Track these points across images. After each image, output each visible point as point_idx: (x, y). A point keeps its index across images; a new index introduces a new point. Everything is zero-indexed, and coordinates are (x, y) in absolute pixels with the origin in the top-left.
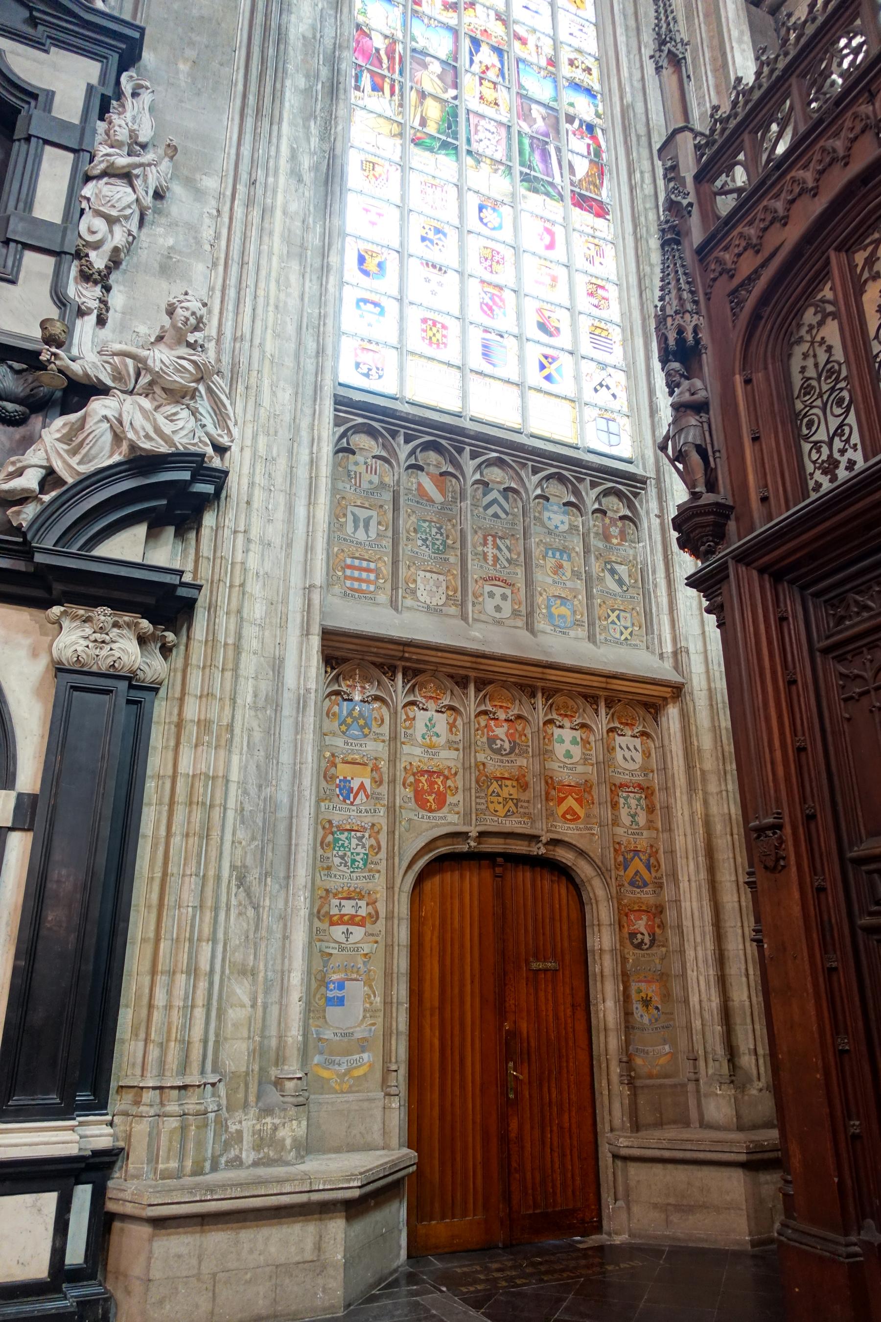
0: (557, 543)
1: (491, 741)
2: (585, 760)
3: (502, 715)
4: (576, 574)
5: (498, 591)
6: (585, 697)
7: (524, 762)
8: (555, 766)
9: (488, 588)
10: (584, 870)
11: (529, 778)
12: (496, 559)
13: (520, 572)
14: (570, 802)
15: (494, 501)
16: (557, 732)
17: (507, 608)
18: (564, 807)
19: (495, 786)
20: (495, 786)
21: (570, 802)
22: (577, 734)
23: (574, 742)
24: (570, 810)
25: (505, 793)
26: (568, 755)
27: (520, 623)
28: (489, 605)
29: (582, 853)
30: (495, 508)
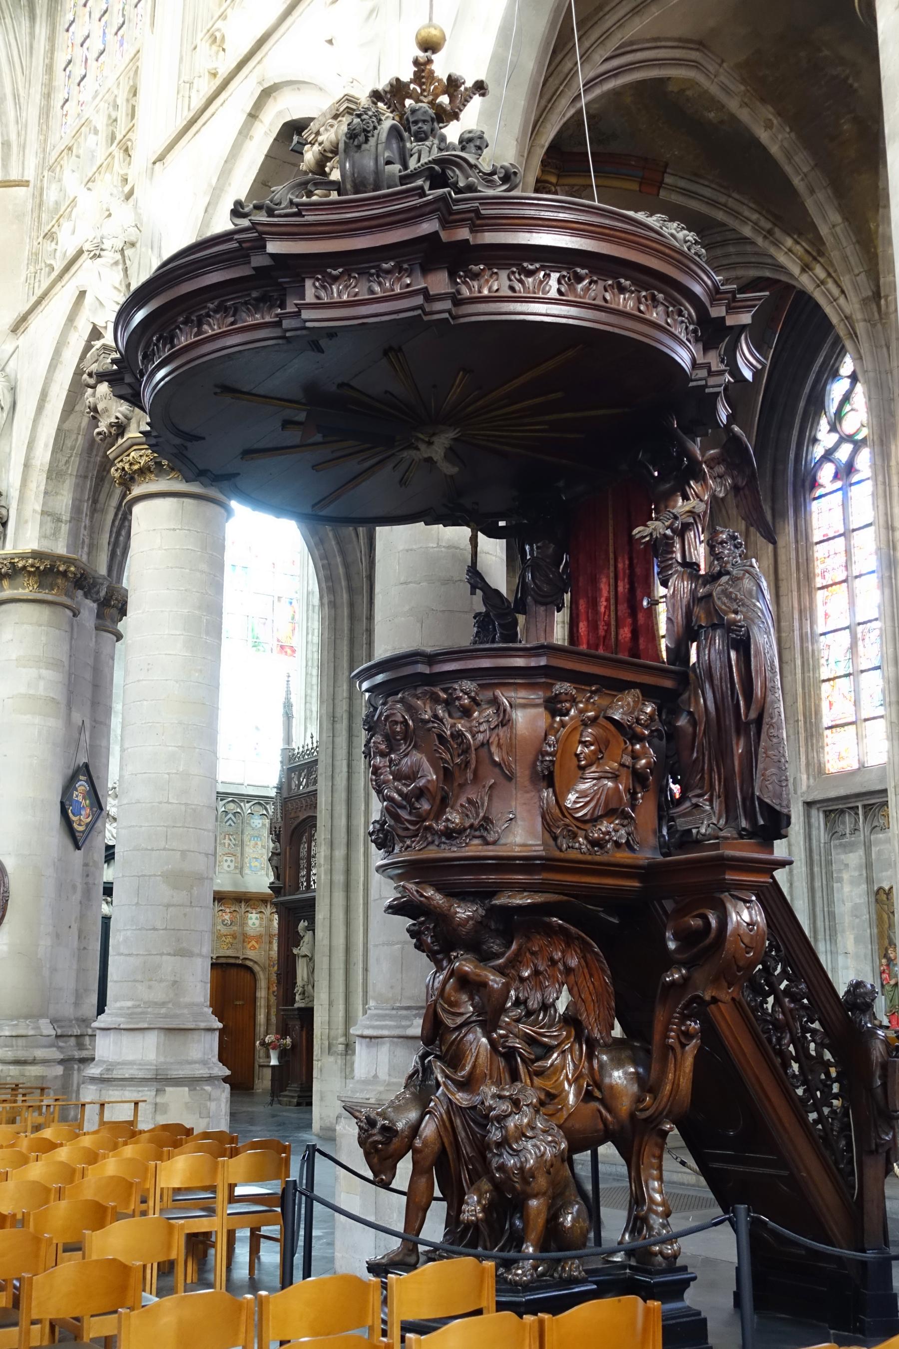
0: (256, 833)
1: (223, 921)
2: (261, 925)
3: (228, 910)
4: (263, 847)
5: (229, 859)
6: (262, 901)
7: (235, 928)
8: (248, 929)
9: (225, 858)
10: (256, 968)
11: (237, 934)
12: (229, 845)
13: (239, 849)
14: (253, 943)
15: (230, 818)
16: (250, 915)
17: (232, 865)
18: (251, 944)
19: (224, 938)
20: (224, 938)
21: (253, 943)
22: (258, 915)
23: (257, 919)
24: (253, 946)
25: (227, 941)
26: (254, 924)
27: (238, 871)
28: (226, 865)
29: (255, 962)
30: (230, 822)
